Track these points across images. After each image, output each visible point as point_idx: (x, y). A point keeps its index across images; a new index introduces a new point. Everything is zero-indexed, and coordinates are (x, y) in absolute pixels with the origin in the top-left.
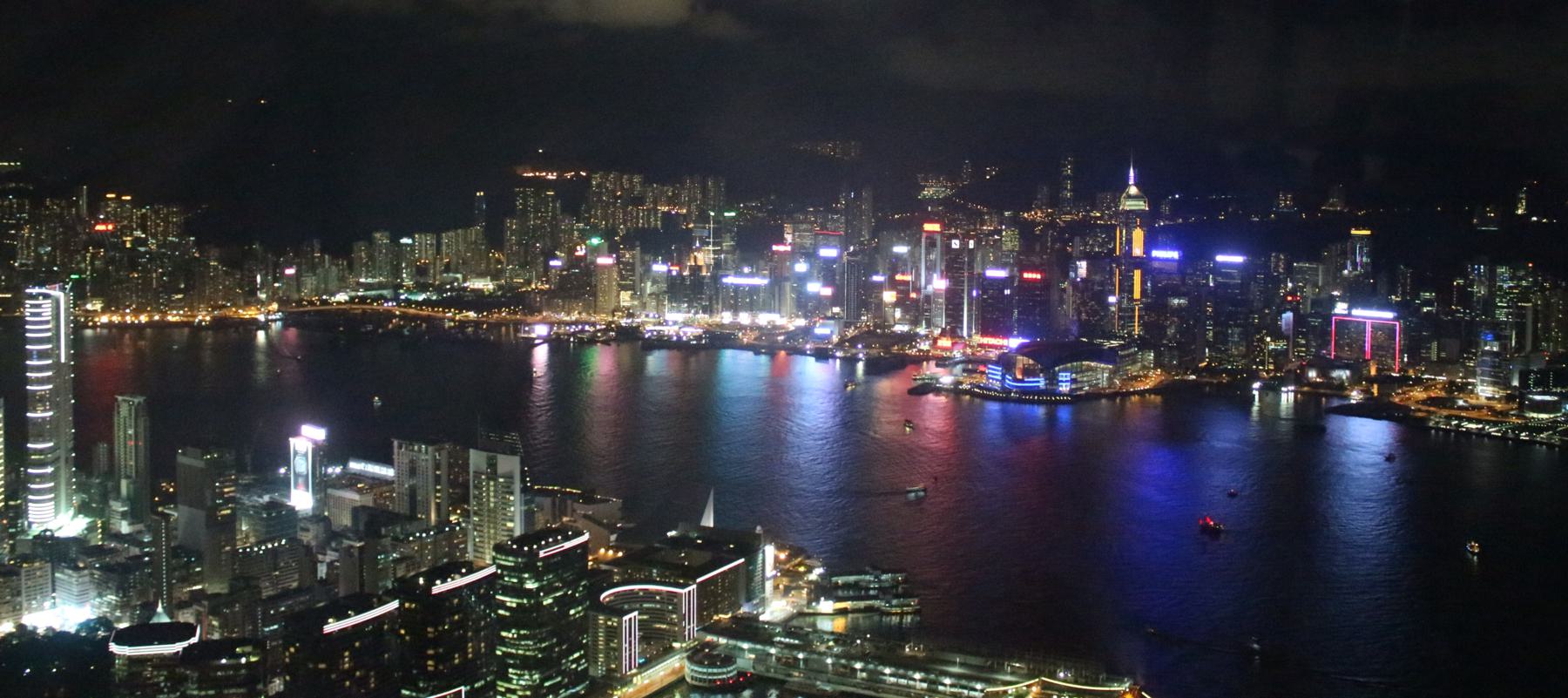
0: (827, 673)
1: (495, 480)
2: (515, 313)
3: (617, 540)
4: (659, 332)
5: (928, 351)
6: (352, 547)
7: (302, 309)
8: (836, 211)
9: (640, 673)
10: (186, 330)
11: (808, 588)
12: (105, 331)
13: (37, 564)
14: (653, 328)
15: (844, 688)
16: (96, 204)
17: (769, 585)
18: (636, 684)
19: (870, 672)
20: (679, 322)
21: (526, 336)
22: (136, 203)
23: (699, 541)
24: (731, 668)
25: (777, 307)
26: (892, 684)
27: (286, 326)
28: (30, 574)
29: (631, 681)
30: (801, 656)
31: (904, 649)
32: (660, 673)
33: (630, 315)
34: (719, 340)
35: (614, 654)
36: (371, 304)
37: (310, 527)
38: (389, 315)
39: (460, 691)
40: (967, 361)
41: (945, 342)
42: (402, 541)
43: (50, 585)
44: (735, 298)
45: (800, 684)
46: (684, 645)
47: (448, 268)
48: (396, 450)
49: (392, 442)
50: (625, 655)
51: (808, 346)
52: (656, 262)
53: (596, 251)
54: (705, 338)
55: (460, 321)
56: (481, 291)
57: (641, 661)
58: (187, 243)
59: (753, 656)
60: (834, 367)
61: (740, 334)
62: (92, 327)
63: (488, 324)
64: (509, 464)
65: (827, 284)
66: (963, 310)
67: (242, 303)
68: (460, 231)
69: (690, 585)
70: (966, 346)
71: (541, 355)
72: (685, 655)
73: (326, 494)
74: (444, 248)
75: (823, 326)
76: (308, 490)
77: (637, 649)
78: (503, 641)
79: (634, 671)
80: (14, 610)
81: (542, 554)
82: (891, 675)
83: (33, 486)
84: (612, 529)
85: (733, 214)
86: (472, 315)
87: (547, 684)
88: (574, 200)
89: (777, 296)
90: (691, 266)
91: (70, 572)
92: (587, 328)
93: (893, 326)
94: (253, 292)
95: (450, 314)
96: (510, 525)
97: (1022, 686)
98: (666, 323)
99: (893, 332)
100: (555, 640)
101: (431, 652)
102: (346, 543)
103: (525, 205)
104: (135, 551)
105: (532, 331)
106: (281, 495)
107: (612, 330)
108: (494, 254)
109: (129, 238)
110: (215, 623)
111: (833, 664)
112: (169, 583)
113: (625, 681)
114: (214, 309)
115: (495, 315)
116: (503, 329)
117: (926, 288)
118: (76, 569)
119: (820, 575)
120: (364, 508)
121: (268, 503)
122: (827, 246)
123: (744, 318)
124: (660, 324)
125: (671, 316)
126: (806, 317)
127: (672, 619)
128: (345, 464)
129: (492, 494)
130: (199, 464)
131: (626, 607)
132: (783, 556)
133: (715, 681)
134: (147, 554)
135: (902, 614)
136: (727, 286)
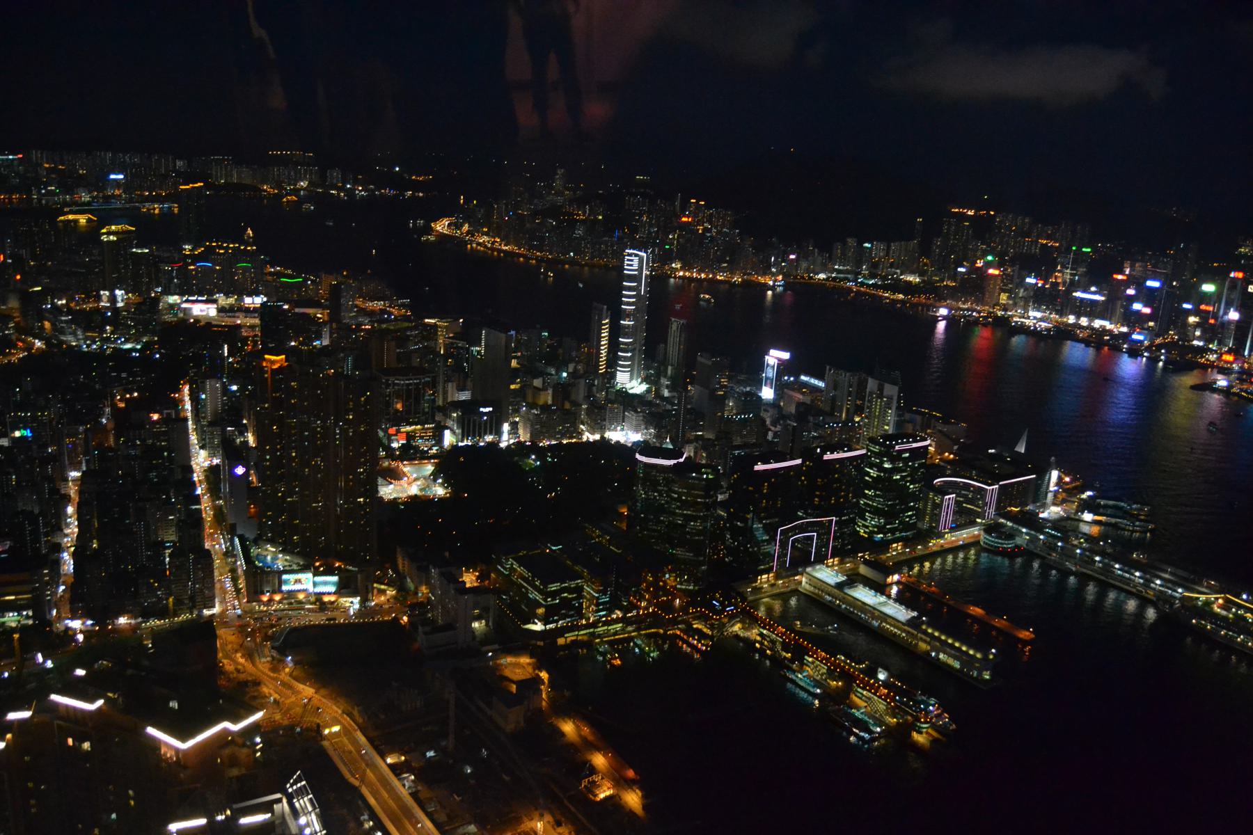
0: (1075, 558)
1: (882, 399)
2: (929, 299)
3: (958, 449)
4: (1022, 322)
5: (1214, 362)
6: (790, 425)
7: (797, 280)
8: (1167, 256)
9: (950, 532)
10: (727, 286)
11: (1078, 503)
12: (681, 281)
13: (616, 406)
14: (1018, 320)
15: (1085, 571)
16: (685, 205)
17: (1050, 496)
18: (946, 539)
19: (1105, 564)
20: (1035, 318)
21: (933, 314)
22: (707, 206)
23: (1009, 459)
24: (1011, 542)
25: (1109, 315)
26: (1119, 575)
27: (785, 290)
28: (612, 410)
29: (944, 536)
30: (1060, 544)
31: (1133, 554)
32: (965, 535)
33: (1005, 310)
34: (1064, 334)
35: (936, 518)
36: (840, 282)
37: (769, 409)
38: (850, 290)
39: (833, 519)
40: (1242, 371)
41: (1230, 358)
42: (821, 427)
43: (621, 418)
44: (1080, 307)
45: (1055, 561)
46: (984, 521)
47: (892, 265)
48: (827, 372)
49: (826, 367)
50: (943, 519)
51: (1125, 346)
52: (1030, 277)
53: (988, 265)
54: (1053, 331)
55: (893, 299)
56: (911, 282)
57: (953, 525)
58: (734, 233)
59: (1028, 538)
60: (1141, 362)
61: (1078, 331)
62: (675, 277)
63: (911, 304)
64: (891, 390)
65: (1145, 306)
66: (1247, 337)
67: (761, 272)
68: (903, 243)
69: (994, 485)
70: (1244, 362)
71: (941, 326)
72: (983, 527)
73: (783, 392)
74: (891, 252)
75: (1139, 333)
76: (772, 388)
77: (950, 518)
78: (866, 496)
79: (947, 530)
80: (601, 428)
81: (897, 448)
82: (1119, 569)
83: (620, 362)
84: (956, 442)
85: (1089, 250)
86: (901, 296)
87: (888, 527)
88: (983, 230)
89: (1109, 312)
90: (1052, 282)
91: (633, 413)
92: (974, 314)
93: (1192, 341)
94: (769, 266)
95: (887, 295)
96: (886, 427)
97: (1212, 597)
98: (1028, 318)
99: (1193, 346)
100: (897, 501)
101: (818, 493)
102: (789, 422)
103: (948, 229)
104: (669, 407)
105: (935, 312)
106: (757, 389)
107: (991, 317)
108: (923, 260)
109: (701, 227)
110: (704, 455)
111: (1080, 554)
112: (683, 428)
113: (941, 536)
114: (744, 275)
115: (916, 299)
116: (920, 308)
117: (1222, 317)
118: (636, 411)
119: (1089, 496)
120: (803, 403)
121: (747, 392)
122: (1154, 279)
123: (1084, 321)
124: (1024, 318)
125: (1032, 313)
126: (1128, 326)
127: (978, 504)
128: (797, 377)
129: (878, 407)
130: (710, 363)
131: (950, 490)
132: (1067, 479)
133: (999, 547)
134: (675, 410)
135: (1133, 531)
136: (1076, 298)
